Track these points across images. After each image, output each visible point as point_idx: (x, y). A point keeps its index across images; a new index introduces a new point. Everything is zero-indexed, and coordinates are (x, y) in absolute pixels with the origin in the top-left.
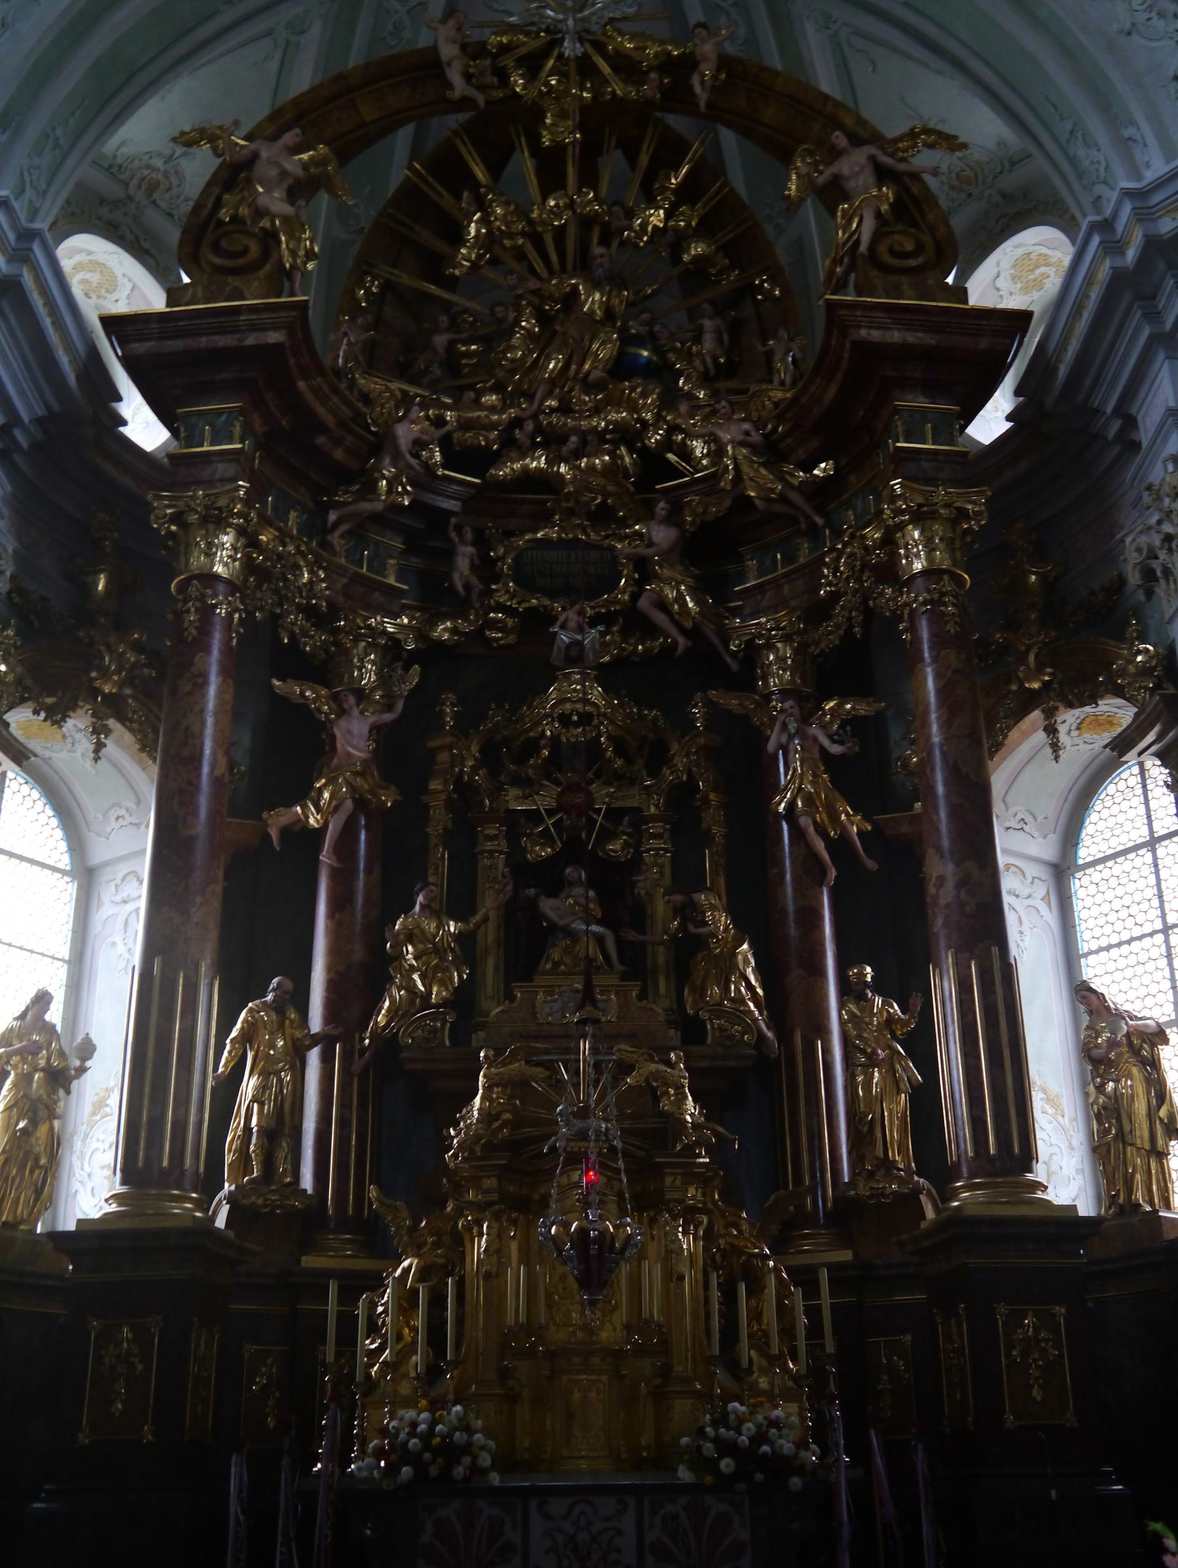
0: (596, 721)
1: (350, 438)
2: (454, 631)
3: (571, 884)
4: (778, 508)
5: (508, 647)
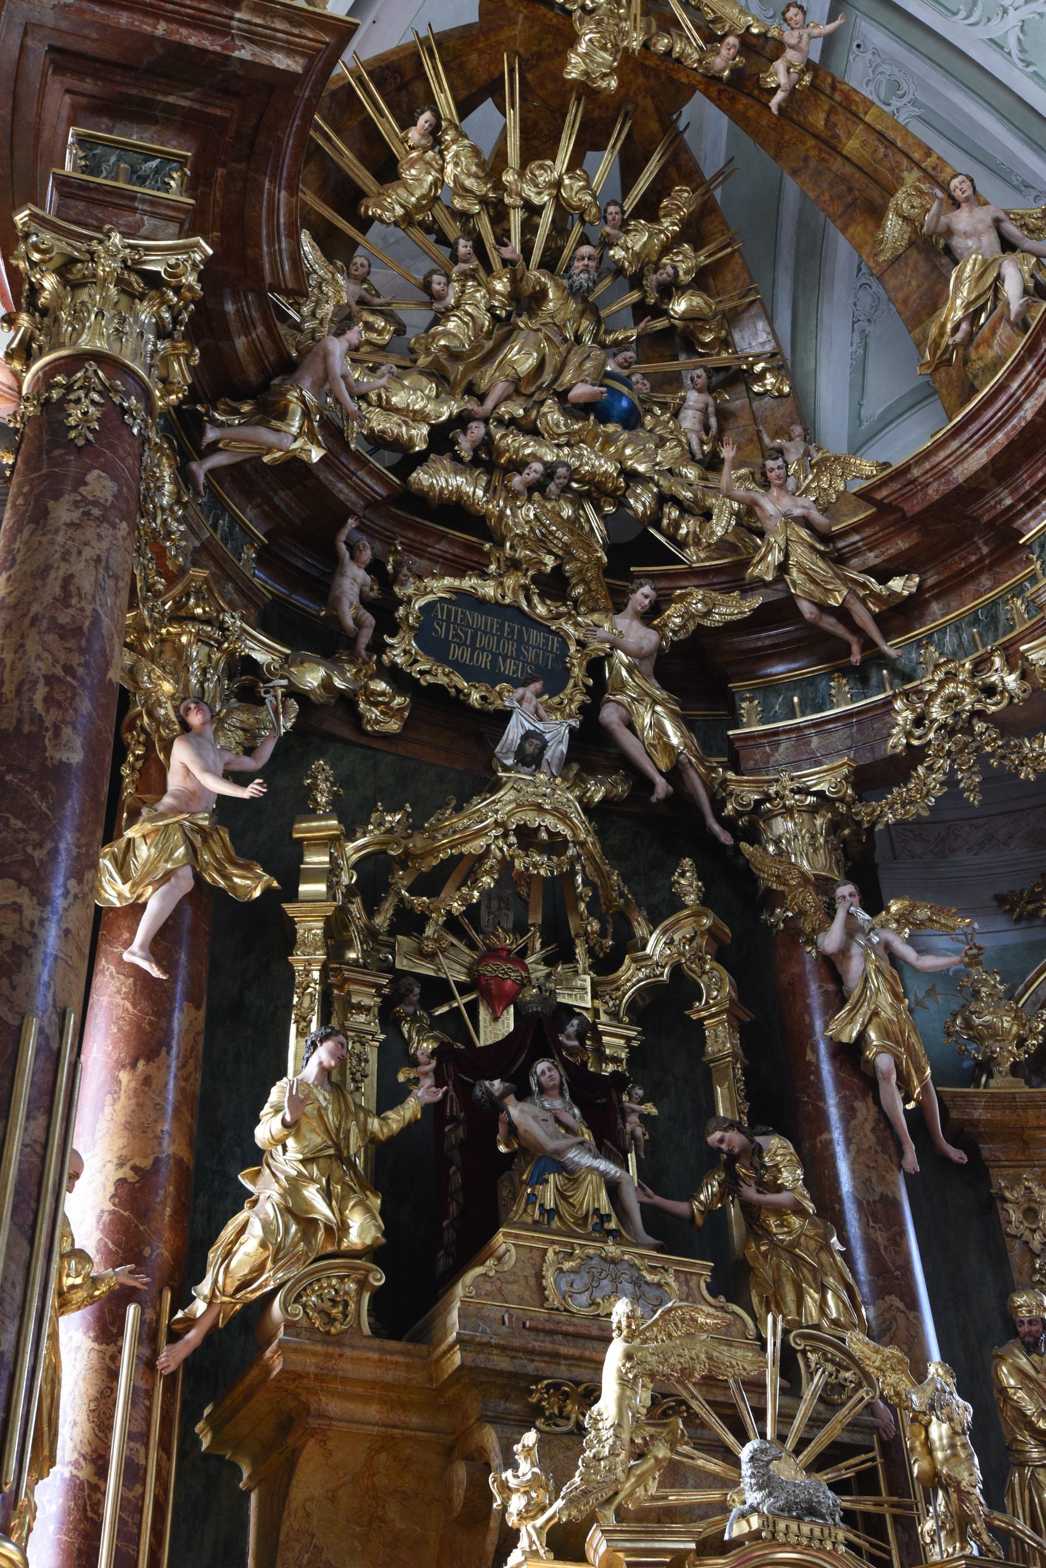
0: (571, 852)
1: (260, 329)
2: (327, 684)
3: (543, 1090)
4: (830, 623)
5: (386, 737)
